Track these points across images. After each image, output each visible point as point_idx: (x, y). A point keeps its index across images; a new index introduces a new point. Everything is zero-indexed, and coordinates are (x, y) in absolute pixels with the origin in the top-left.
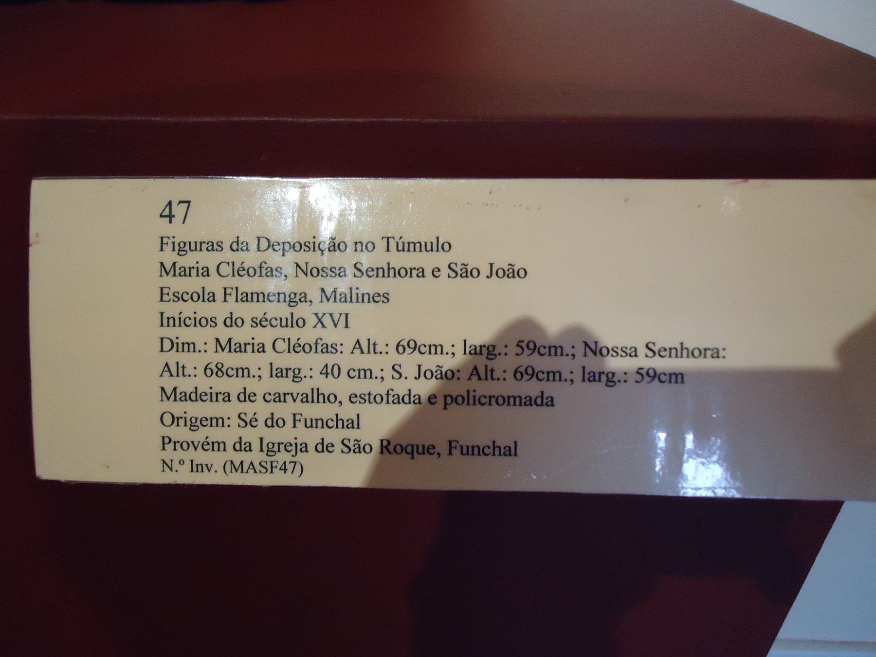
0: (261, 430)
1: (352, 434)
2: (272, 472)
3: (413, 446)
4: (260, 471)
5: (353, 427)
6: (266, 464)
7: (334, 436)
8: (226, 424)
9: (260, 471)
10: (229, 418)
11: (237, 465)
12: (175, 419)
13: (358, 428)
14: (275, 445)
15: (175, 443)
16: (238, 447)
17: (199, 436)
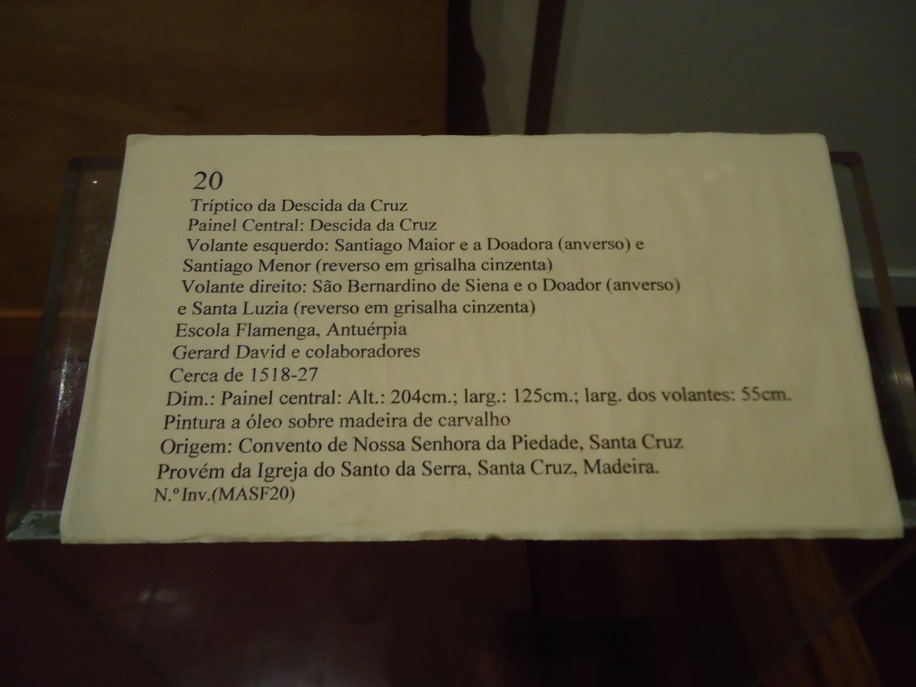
8: (226, 450)
10: (230, 444)
12: (176, 447)
14: (274, 470)
15: (172, 471)
17: (197, 462)
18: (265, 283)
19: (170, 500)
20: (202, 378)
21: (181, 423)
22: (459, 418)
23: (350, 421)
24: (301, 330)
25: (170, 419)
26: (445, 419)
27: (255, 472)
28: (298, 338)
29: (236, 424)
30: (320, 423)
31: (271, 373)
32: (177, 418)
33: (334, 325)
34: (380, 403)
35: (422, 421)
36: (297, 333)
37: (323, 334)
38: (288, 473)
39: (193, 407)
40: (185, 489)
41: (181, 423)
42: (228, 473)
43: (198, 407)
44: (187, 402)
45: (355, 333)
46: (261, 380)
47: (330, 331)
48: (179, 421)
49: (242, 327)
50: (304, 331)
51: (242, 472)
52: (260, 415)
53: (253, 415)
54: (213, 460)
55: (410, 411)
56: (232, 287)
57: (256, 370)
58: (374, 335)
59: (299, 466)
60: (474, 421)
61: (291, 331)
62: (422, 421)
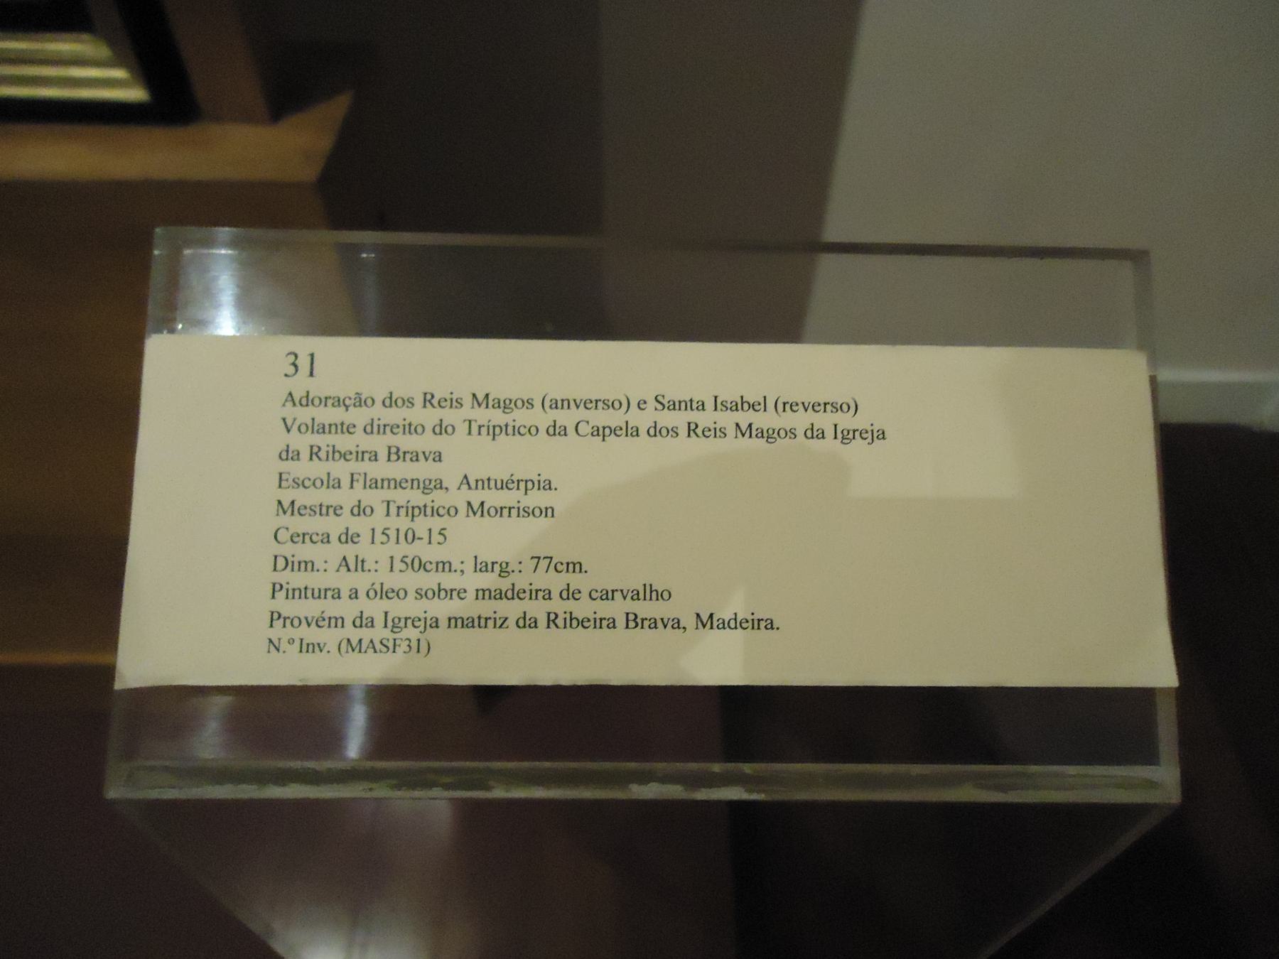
18: (382, 423)
19: (284, 652)
20: (311, 538)
21: (290, 593)
22: (613, 591)
23: (487, 593)
24: (427, 482)
25: (278, 587)
26: (597, 591)
27: (379, 621)
28: (423, 492)
29: (354, 595)
30: (451, 595)
31: (392, 534)
32: (285, 586)
33: (466, 477)
34: (517, 572)
35: (570, 594)
36: (422, 485)
37: (453, 488)
38: (417, 624)
39: (302, 574)
41: (290, 593)
42: (348, 623)
43: (309, 574)
44: (296, 567)
45: (491, 487)
46: (382, 543)
47: (461, 484)
48: (288, 590)
49: (356, 477)
50: (430, 484)
51: (363, 621)
52: (382, 584)
53: (373, 584)
54: (332, 608)
55: (556, 582)
56: (342, 427)
57: (376, 531)
58: (514, 490)
59: (429, 616)
60: (630, 595)
61: (416, 483)
62: (570, 594)
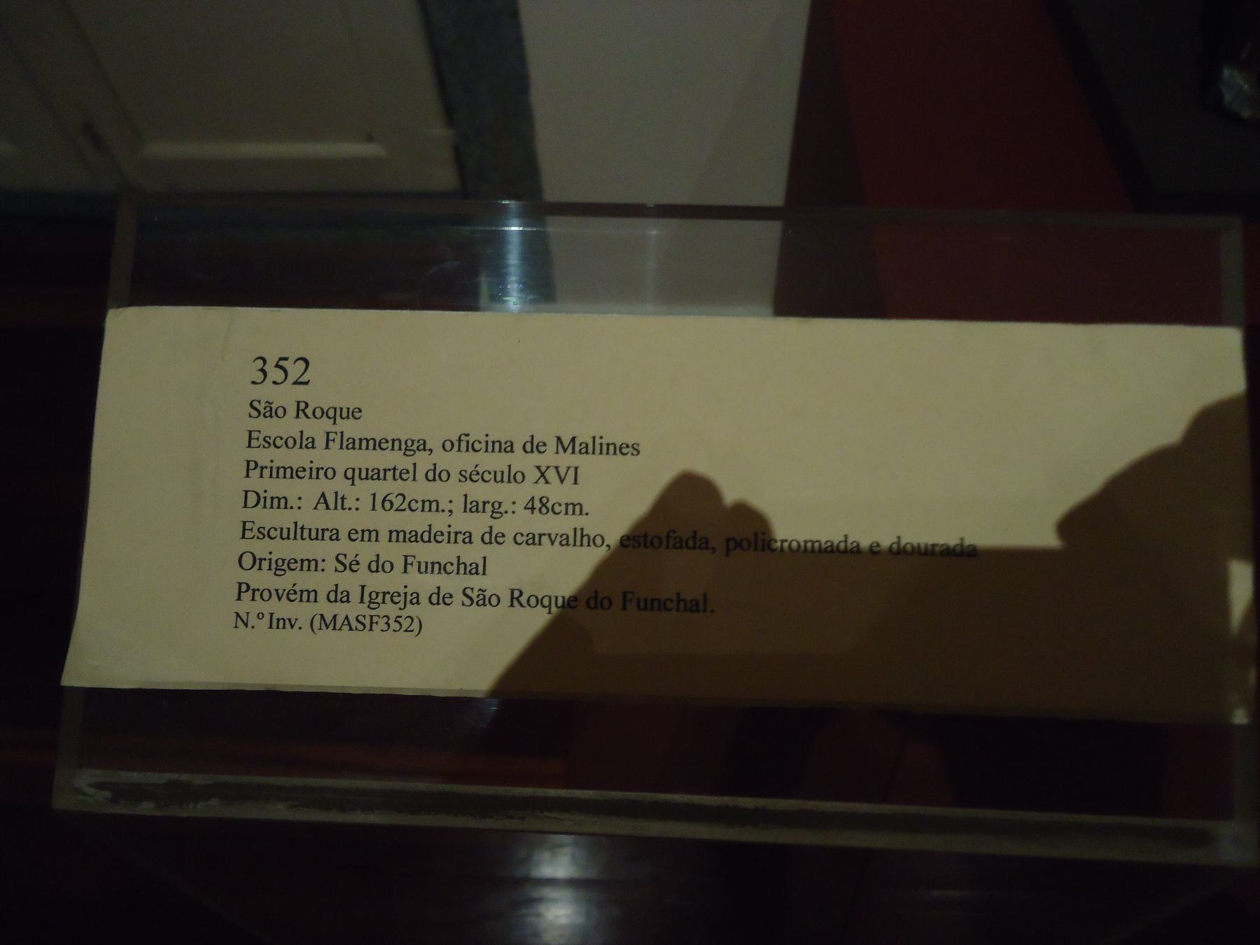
0: (363, 576)
1: (476, 582)
2: (371, 630)
3: (550, 598)
4: (356, 627)
5: (477, 573)
6: (365, 619)
7: (453, 584)
9: (356, 627)
11: (329, 618)
13: (484, 574)
16: (332, 597)
40: (272, 614)
